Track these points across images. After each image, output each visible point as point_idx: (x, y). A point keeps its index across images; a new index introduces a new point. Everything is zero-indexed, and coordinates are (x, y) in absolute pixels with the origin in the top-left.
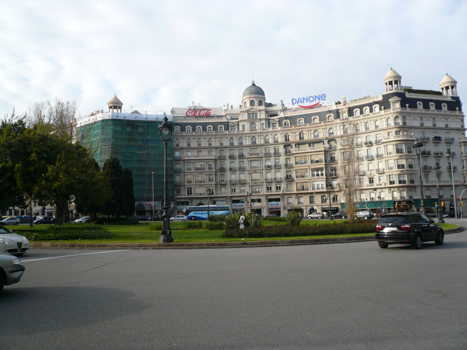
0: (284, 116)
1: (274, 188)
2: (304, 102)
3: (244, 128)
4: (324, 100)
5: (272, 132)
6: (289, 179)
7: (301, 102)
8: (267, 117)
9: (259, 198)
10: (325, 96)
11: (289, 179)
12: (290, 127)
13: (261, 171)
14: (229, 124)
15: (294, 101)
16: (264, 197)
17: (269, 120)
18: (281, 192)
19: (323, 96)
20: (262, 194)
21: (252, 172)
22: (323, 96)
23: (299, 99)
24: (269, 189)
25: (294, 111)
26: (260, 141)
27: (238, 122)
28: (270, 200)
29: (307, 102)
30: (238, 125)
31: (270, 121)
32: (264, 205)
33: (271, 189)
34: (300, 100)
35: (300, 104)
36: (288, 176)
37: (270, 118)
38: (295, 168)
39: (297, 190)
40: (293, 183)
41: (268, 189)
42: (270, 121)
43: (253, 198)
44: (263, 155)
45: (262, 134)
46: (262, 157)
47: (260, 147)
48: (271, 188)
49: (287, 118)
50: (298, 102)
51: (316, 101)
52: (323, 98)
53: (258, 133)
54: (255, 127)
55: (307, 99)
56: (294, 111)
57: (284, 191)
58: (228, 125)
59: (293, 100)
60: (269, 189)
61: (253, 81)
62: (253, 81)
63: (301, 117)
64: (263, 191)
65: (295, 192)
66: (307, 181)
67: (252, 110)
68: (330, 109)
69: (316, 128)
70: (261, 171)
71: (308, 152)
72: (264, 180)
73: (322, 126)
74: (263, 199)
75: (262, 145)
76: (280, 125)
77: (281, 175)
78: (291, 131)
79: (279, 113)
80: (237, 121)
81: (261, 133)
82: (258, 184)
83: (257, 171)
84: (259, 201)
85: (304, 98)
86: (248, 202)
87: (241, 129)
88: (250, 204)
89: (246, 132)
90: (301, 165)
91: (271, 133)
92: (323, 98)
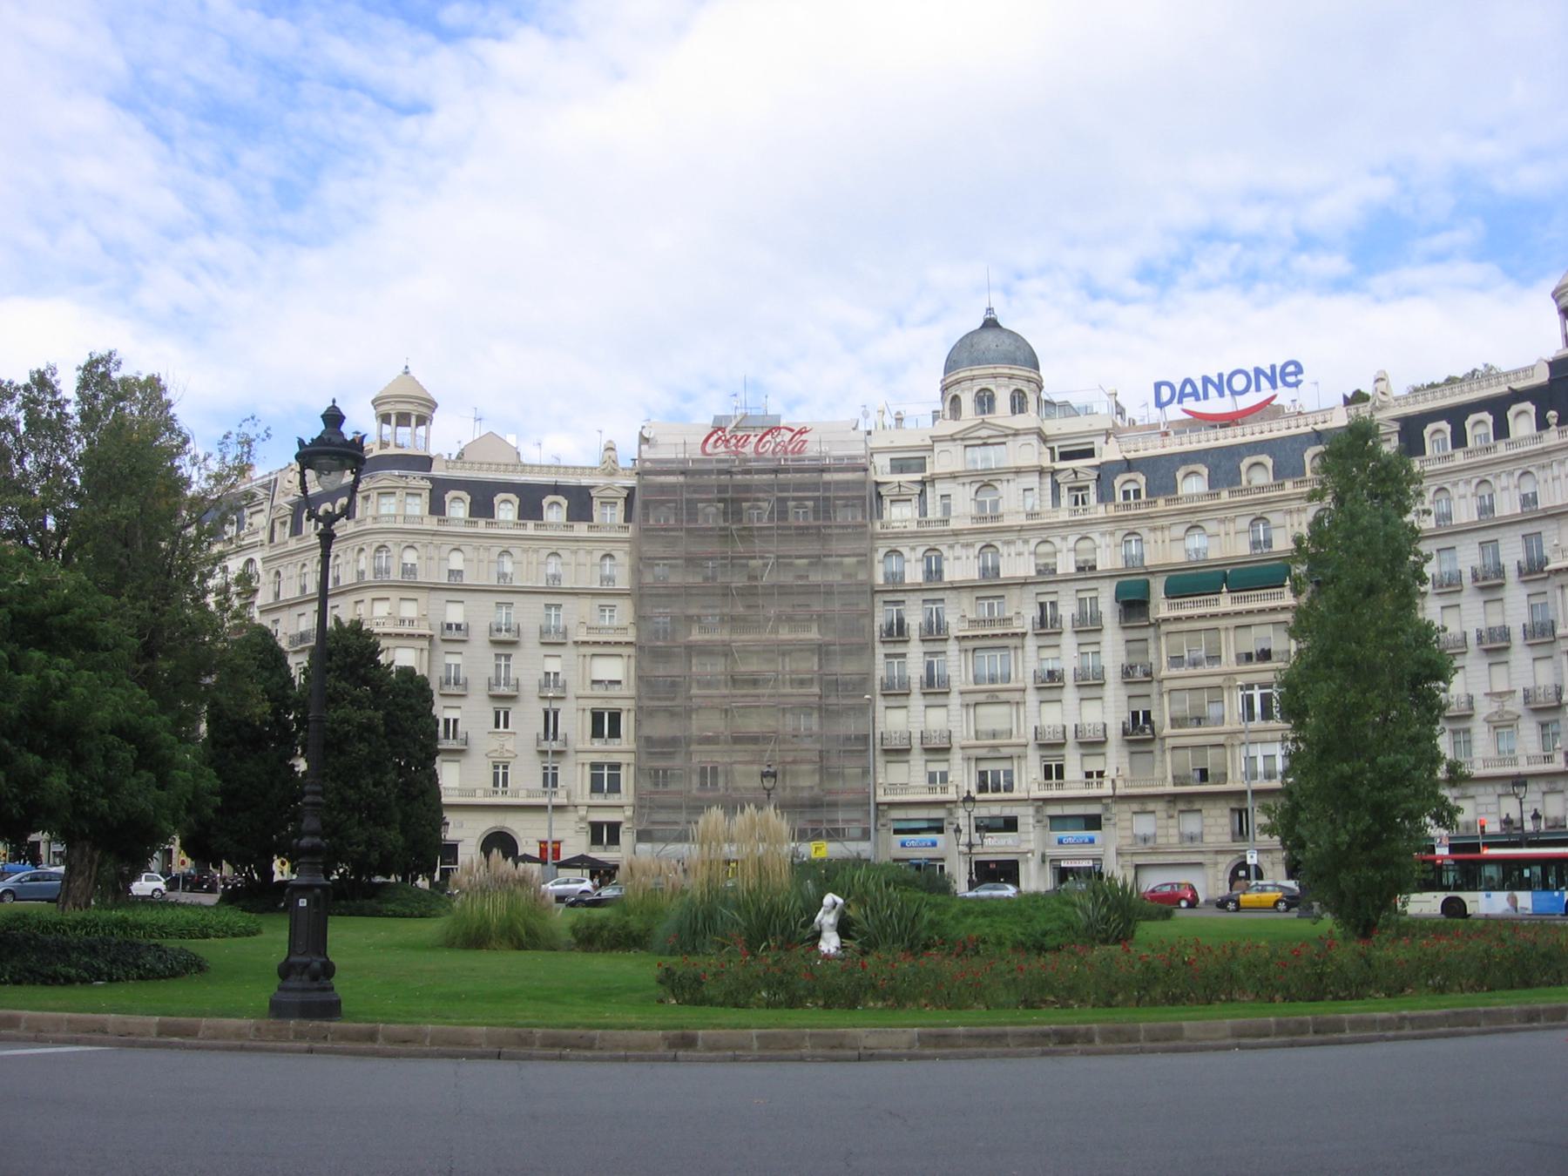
0: (1119, 457)
1: (1073, 771)
2: (1206, 397)
3: (947, 509)
4: (1296, 384)
5: (1067, 525)
6: (1143, 730)
7: (1195, 394)
8: (1047, 463)
9: (1008, 811)
10: (1299, 369)
11: (1139, 731)
12: (1147, 503)
13: (1017, 696)
14: (883, 491)
15: (1166, 393)
16: (1031, 810)
17: (1054, 472)
18: (1106, 789)
19: (1291, 369)
20: (1024, 795)
21: (982, 697)
22: (1291, 369)
23: (1188, 381)
24: (1054, 772)
25: (1166, 434)
26: (1017, 563)
27: (923, 483)
28: (1058, 822)
29: (1221, 395)
30: (922, 493)
31: (1060, 478)
32: (1032, 846)
33: (1060, 775)
34: (1188, 389)
35: (1190, 404)
36: (1135, 715)
37: (1059, 465)
38: (1167, 685)
39: (1177, 780)
40: (1156, 747)
41: (1048, 775)
42: (1060, 478)
43: (983, 811)
44: (1028, 628)
45: (1025, 535)
46: (1024, 635)
47: (1015, 592)
48: (1060, 769)
49: (1129, 465)
50: (1182, 395)
51: (1258, 389)
52: (1291, 379)
53: (1009, 529)
54: (995, 504)
55: (1222, 385)
56: (1166, 434)
57: (1119, 783)
58: (879, 496)
59: (1158, 386)
60: (1054, 772)
61: (990, 310)
62: (990, 310)
63: (1195, 462)
64: (1029, 780)
65: (1170, 788)
66: (1221, 739)
67: (984, 433)
68: (1319, 427)
69: (1258, 510)
70: (1017, 696)
71: (1226, 615)
72: (1031, 736)
73: (1286, 499)
74: (1026, 816)
75: (1024, 583)
76: (1105, 496)
77: (1108, 712)
78: (1151, 523)
79: (1098, 443)
80: (918, 477)
81: (1021, 529)
82: (1005, 752)
83: (1004, 696)
84: (1010, 825)
85: (1206, 380)
86: (958, 830)
87: (935, 512)
88: (964, 839)
89: (954, 525)
90: (1191, 671)
91: (1064, 532)
92: (1291, 379)
